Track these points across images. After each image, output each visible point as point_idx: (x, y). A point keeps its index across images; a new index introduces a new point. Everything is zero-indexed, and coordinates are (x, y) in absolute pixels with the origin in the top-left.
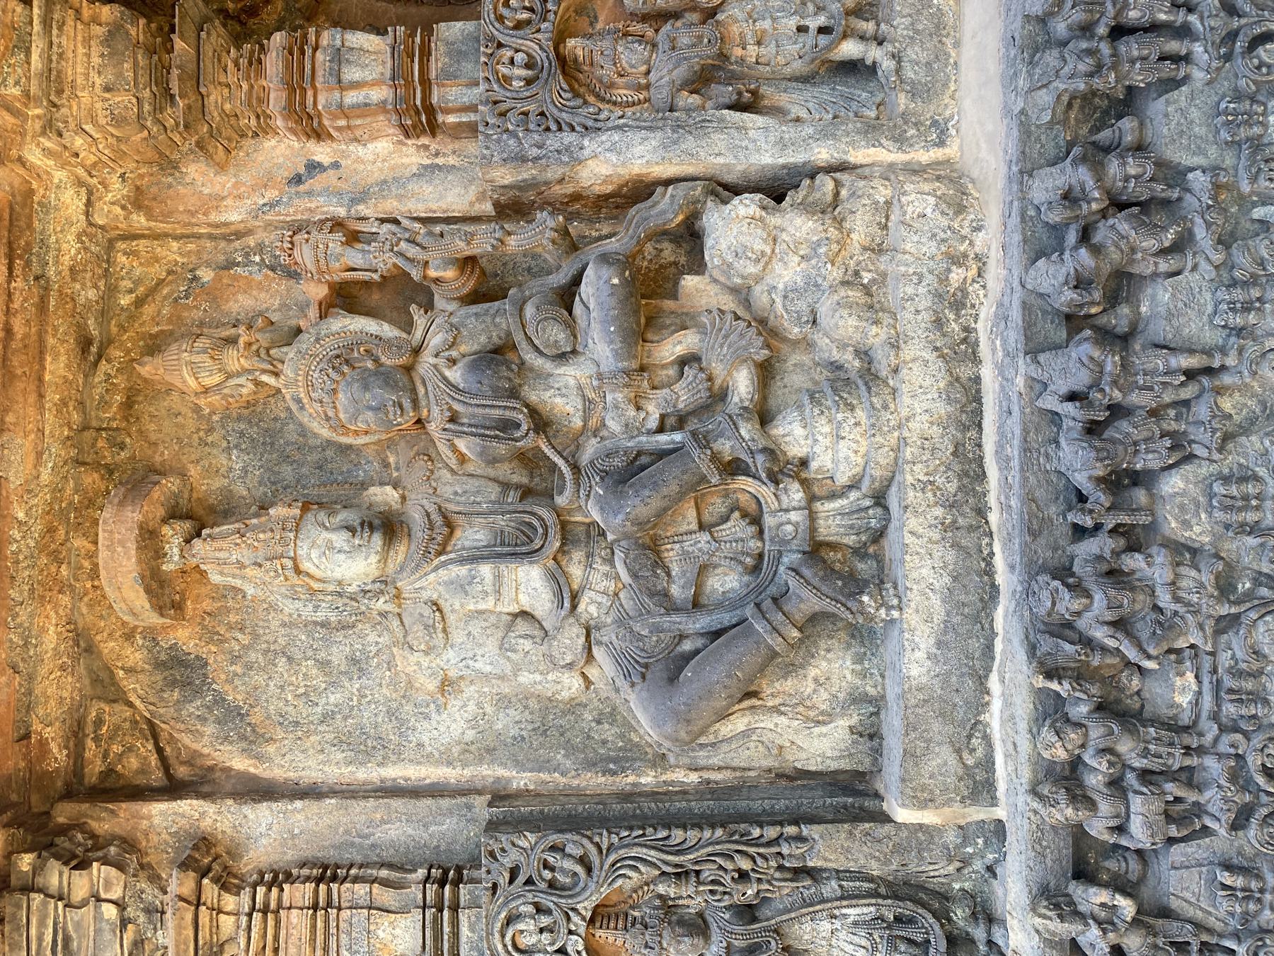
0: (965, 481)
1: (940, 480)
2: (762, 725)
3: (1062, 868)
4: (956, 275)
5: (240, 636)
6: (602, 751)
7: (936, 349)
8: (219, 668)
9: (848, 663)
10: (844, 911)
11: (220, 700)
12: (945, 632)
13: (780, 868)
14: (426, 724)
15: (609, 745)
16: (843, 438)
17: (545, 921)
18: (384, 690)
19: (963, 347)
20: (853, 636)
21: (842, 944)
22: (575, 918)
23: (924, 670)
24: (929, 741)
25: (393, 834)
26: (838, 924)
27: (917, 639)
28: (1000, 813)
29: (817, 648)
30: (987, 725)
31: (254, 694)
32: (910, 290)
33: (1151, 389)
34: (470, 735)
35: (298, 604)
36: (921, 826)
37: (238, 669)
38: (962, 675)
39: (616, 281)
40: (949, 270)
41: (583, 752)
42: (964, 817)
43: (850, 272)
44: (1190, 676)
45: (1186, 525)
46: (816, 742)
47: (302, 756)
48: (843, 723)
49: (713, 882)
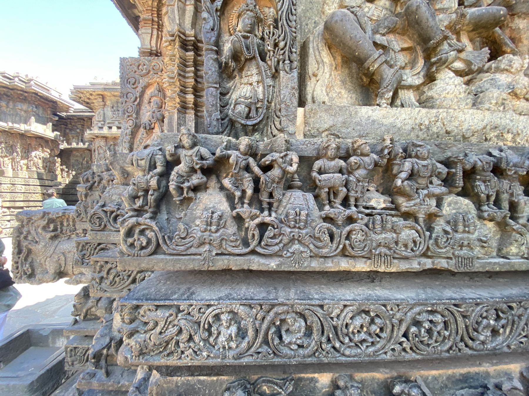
0: (436, 136)
1: (438, 124)
2: (326, 68)
4: (509, 136)
7: (487, 125)
13: (278, 62)
15: (306, 27)
16: (456, 87)
19: (484, 138)
21: (246, 88)
23: (364, 115)
24: (335, 116)
26: (255, 84)
27: (377, 111)
29: (352, 94)
32: (508, 116)
33: (510, 188)
36: (296, 116)
39: (502, 12)
40: (512, 133)
43: (504, 101)
44: (383, 206)
45: (449, 205)
48: (326, 99)
49: (273, 34)
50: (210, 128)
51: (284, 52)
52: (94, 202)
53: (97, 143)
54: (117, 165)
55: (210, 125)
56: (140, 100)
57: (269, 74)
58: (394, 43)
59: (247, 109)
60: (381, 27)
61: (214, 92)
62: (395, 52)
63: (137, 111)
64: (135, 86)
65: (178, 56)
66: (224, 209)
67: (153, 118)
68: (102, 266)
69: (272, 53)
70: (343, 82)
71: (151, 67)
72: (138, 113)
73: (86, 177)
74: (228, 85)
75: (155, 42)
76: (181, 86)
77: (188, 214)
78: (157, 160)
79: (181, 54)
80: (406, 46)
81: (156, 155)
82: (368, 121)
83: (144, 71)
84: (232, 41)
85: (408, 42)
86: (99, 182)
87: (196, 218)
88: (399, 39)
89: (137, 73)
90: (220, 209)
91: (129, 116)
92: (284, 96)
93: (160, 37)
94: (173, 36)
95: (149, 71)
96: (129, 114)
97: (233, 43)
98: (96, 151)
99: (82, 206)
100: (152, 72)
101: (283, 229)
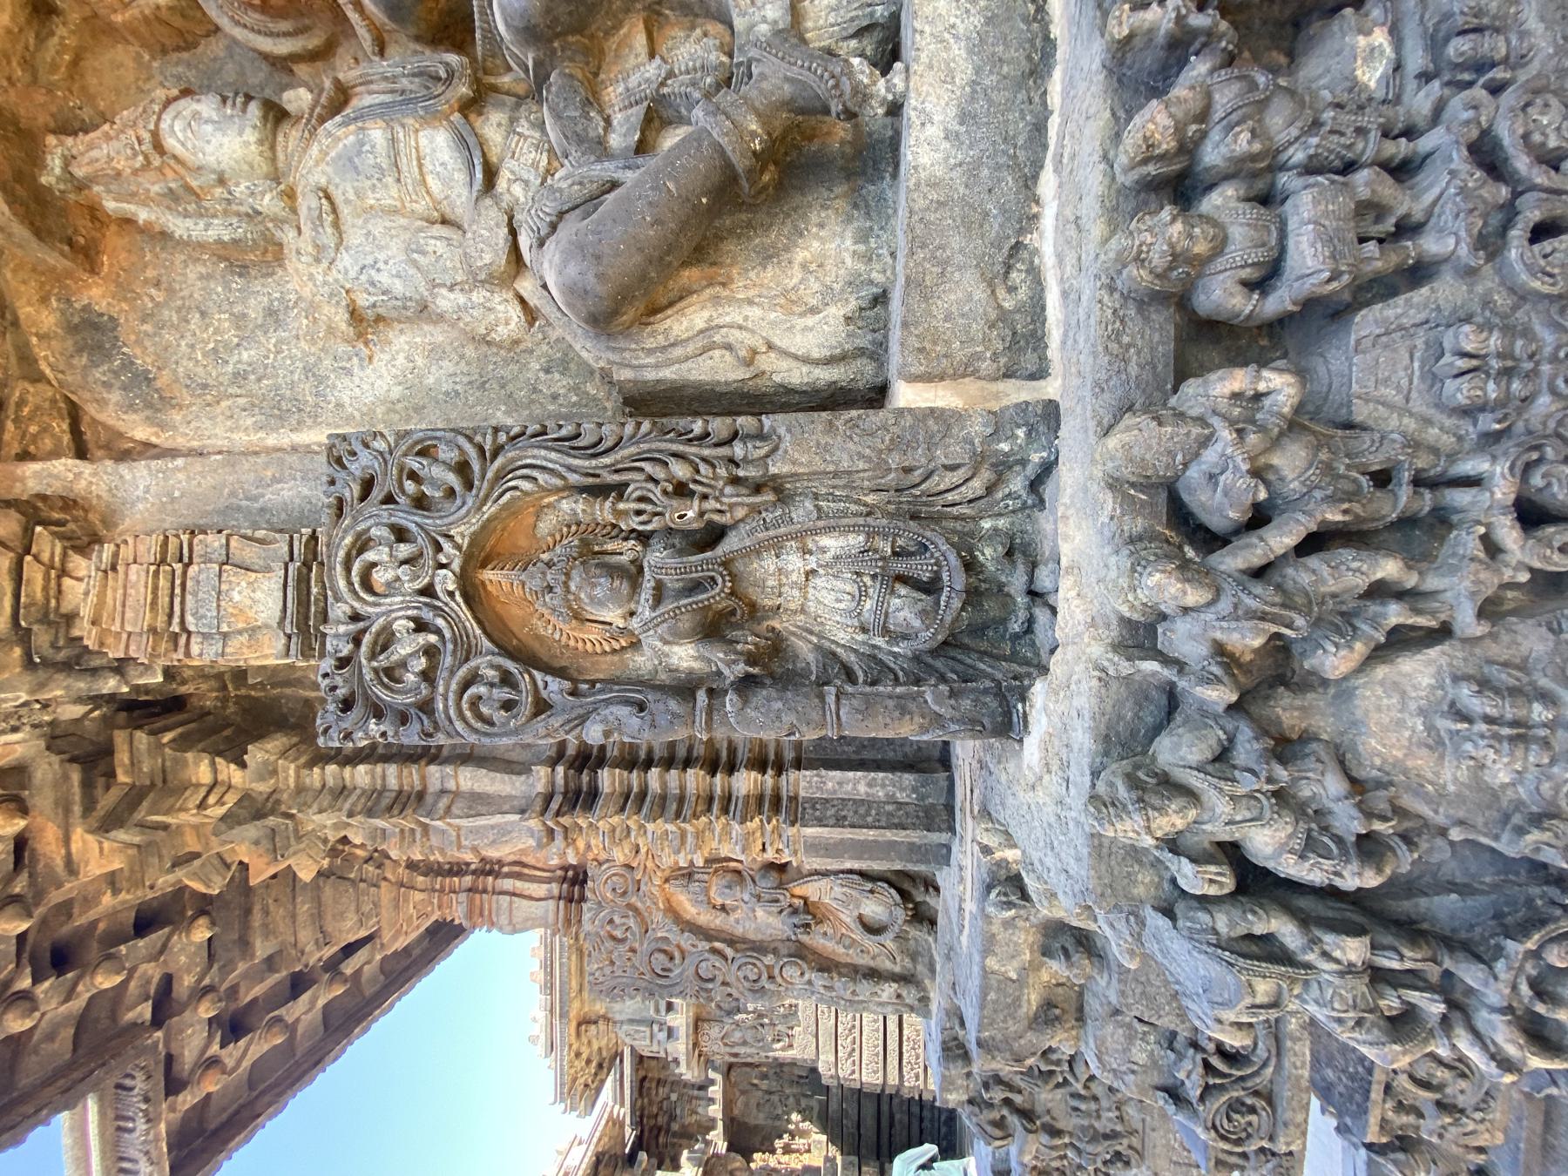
2: (728, 319)
3: (1155, 375)
5: (153, 291)
6: (551, 408)
8: (130, 327)
9: (848, 242)
10: (826, 541)
11: (129, 364)
12: (973, 98)
13: (735, 481)
14: (346, 381)
15: (561, 401)
17: (404, 550)
18: (303, 344)
20: (855, 206)
22: (447, 546)
24: (945, 263)
25: (286, 493)
27: (928, 107)
28: (1051, 388)
29: (807, 223)
30: (1036, 252)
31: (164, 356)
34: (397, 391)
35: (189, 223)
36: (932, 410)
37: (147, 327)
38: (998, 167)
41: (528, 406)
42: (997, 396)
46: (799, 338)
47: (208, 423)
49: (641, 499)
50: (986, 721)
51: (704, 460)
52: (1076, 1109)
53: (715, 1048)
54: (1022, 1042)
55: (973, 721)
56: (717, 940)
57: (779, 512)
58: (633, 81)
59: (903, 590)
60: (585, 130)
61: (855, 702)
62: (671, 74)
63: (753, 949)
64: (677, 955)
65: (615, 820)
66: (1432, 670)
67: (777, 901)
68: (1400, 1107)
69: (711, 504)
70: (768, 256)
71: (619, 900)
72: (759, 948)
73: (989, 1129)
74: (811, 657)
75: (535, 886)
76: (709, 809)
77: (1461, 814)
78: (1241, 930)
79: (612, 810)
80: (640, 41)
81: (1215, 931)
82: (964, 138)
83: (631, 922)
84: (666, 642)
85: (626, 36)
86: (1010, 1087)
87: (1478, 784)
88: (615, 69)
89: (637, 945)
90: (1433, 688)
91: (771, 977)
92: (861, 456)
93: (517, 869)
94: (551, 832)
95: (630, 906)
96: (765, 976)
97: (676, 637)
98: (735, 1050)
99: (1090, 1148)
100: (634, 900)
101: (1536, 424)
